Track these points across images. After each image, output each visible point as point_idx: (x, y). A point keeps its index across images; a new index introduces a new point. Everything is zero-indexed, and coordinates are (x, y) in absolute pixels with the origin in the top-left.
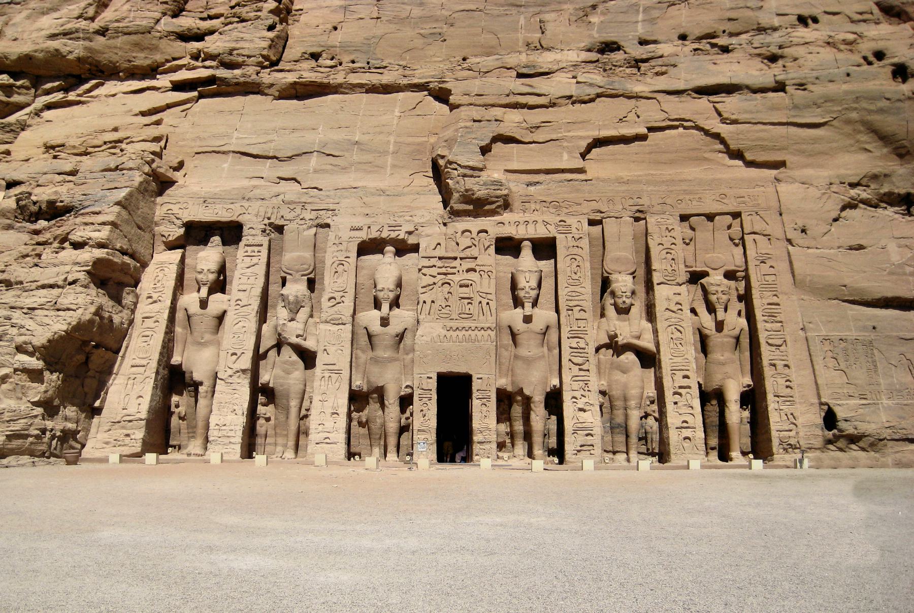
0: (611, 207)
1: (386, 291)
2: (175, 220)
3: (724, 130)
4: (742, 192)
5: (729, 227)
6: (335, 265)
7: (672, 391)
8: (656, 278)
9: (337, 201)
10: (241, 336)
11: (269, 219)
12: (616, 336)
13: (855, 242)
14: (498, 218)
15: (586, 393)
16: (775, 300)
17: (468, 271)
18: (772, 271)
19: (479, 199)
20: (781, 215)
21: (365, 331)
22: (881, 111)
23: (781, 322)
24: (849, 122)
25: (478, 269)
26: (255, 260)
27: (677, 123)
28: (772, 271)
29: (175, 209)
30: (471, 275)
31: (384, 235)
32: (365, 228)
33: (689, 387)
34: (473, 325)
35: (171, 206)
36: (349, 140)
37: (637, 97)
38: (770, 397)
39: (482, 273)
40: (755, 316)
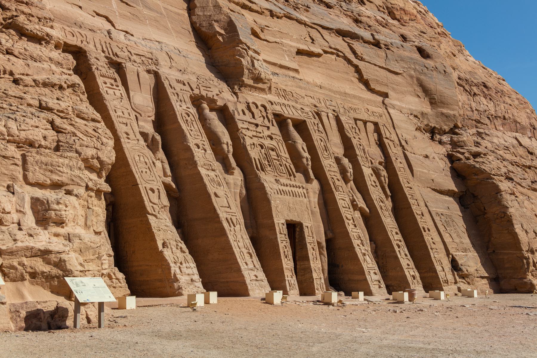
3: (361, 65)
6: (184, 115)
11: (103, 52)
12: (355, 201)
13: (424, 153)
14: (265, 96)
16: (409, 185)
18: (401, 165)
20: (394, 128)
22: (425, 74)
23: (416, 200)
24: (412, 77)
25: (274, 136)
26: (118, 93)
27: (335, 51)
28: (401, 165)
31: (204, 93)
32: (186, 84)
37: (305, 24)
38: (429, 247)
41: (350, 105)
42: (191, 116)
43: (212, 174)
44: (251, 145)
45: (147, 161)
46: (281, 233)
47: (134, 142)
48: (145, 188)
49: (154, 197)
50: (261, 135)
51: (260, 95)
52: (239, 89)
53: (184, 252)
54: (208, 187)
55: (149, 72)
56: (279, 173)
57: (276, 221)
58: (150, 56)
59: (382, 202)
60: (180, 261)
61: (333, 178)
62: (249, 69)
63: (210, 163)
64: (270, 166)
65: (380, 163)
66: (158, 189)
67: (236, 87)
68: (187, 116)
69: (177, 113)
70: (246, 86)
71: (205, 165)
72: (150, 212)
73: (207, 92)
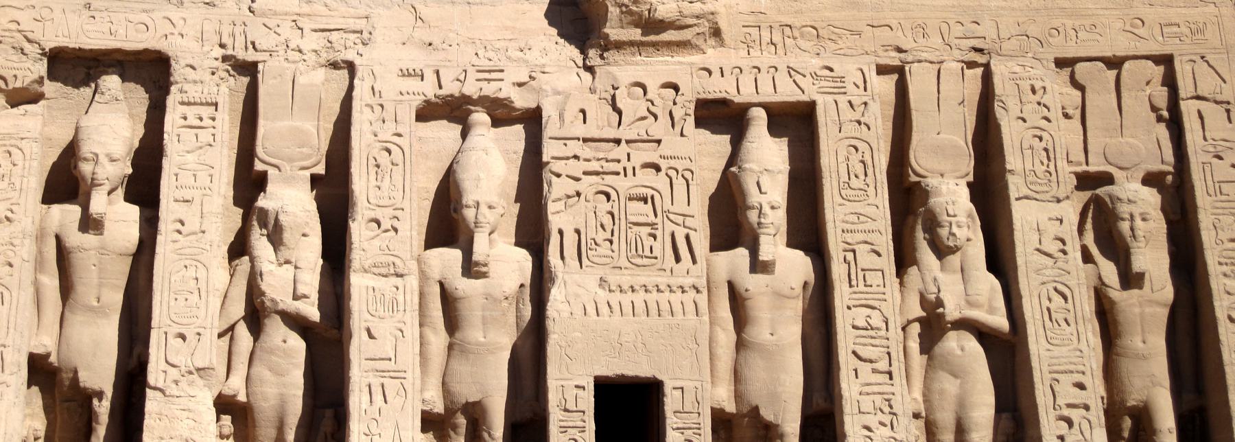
0: (921, 40)
1: (484, 209)
2: (28, 47)
4: (1174, 14)
5: (1148, 83)
7: (1053, 414)
8: (1015, 186)
9: (362, 11)
10: (189, 296)
11: (222, 46)
12: (939, 303)
14: (696, 58)
15: (887, 419)
17: (647, 166)
19: (662, 21)
21: (437, 289)
25: (664, 164)
30: (648, 177)
31: (472, 89)
32: (430, 76)
33: (1087, 408)
34: (662, 280)
35: (17, 15)
39: (672, 173)
40: (1205, 264)
41: (1056, 23)
43: (387, 285)
44: (569, 197)
45: (202, 274)
46: (566, 410)
47: (193, 237)
49: (181, 354)
50: (617, 167)
51: (677, 59)
52: (602, 57)
55: (334, 65)
56: (639, 261)
57: (552, 383)
58: (361, 24)
59: (1065, 298)
61: (854, 251)
62: (621, 5)
64: (611, 242)
65: (1151, 180)
66: (199, 334)
67: (592, 53)
70: (619, 46)
73: (484, 84)
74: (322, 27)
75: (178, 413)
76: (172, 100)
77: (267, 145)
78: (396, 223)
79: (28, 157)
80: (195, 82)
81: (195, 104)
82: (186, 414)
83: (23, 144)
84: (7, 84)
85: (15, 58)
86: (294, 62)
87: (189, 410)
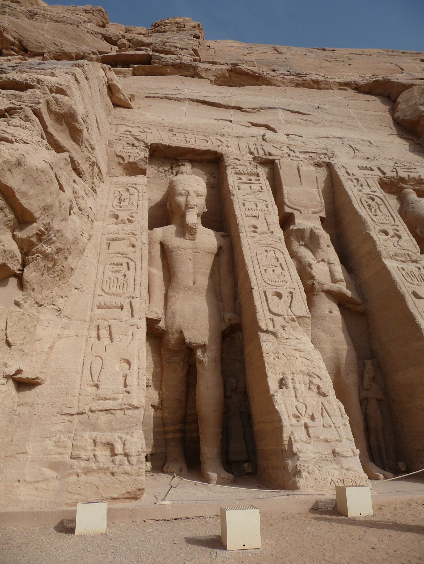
2: (136, 143)
9: (323, 147)
11: (251, 153)
26: (256, 187)
29: (135, 132)
36: (311, 106)
42: (377, 199)
45: (279, 255)
48: (265, 293)
49: (279, 306)
53: (324, 395)
54: (400, 283)
55: (317, 165)
60: (310, 412)
63: (406, 252)
66: (291, 293)
68: (370, 201)
69: (353, 199)
71: (396, 255)
72: (264, 327)
73: (409, 173)
74: (304, 151)
75: (293, 352)
76: (229, 171)
77: (291, 198)
78: (397, 233)
79: (141, 191)
80: (241, 165)
81: (244, 174)
82: (298, 354)
83: (137, 186)
84: (123, 160)
85: (128, 148)
86: (296, 161)
87: (300, 350)
